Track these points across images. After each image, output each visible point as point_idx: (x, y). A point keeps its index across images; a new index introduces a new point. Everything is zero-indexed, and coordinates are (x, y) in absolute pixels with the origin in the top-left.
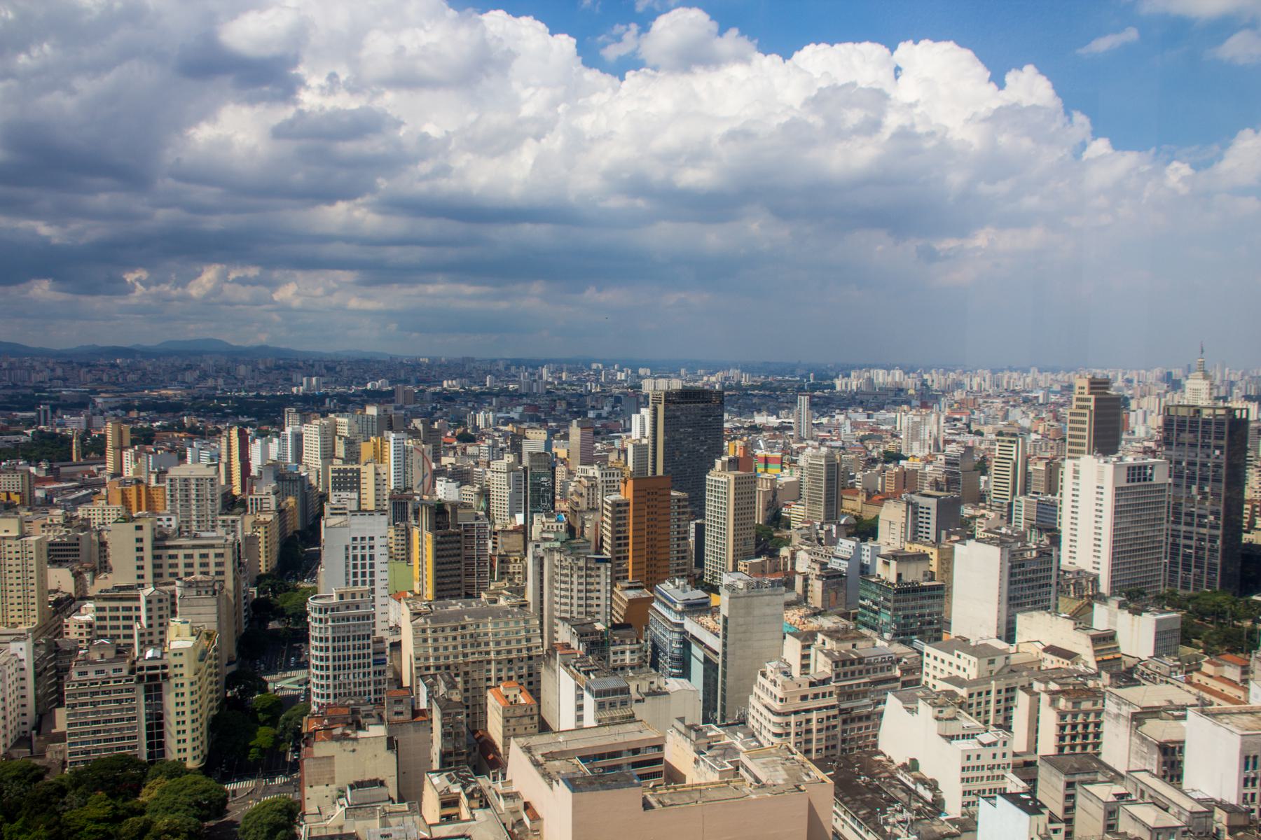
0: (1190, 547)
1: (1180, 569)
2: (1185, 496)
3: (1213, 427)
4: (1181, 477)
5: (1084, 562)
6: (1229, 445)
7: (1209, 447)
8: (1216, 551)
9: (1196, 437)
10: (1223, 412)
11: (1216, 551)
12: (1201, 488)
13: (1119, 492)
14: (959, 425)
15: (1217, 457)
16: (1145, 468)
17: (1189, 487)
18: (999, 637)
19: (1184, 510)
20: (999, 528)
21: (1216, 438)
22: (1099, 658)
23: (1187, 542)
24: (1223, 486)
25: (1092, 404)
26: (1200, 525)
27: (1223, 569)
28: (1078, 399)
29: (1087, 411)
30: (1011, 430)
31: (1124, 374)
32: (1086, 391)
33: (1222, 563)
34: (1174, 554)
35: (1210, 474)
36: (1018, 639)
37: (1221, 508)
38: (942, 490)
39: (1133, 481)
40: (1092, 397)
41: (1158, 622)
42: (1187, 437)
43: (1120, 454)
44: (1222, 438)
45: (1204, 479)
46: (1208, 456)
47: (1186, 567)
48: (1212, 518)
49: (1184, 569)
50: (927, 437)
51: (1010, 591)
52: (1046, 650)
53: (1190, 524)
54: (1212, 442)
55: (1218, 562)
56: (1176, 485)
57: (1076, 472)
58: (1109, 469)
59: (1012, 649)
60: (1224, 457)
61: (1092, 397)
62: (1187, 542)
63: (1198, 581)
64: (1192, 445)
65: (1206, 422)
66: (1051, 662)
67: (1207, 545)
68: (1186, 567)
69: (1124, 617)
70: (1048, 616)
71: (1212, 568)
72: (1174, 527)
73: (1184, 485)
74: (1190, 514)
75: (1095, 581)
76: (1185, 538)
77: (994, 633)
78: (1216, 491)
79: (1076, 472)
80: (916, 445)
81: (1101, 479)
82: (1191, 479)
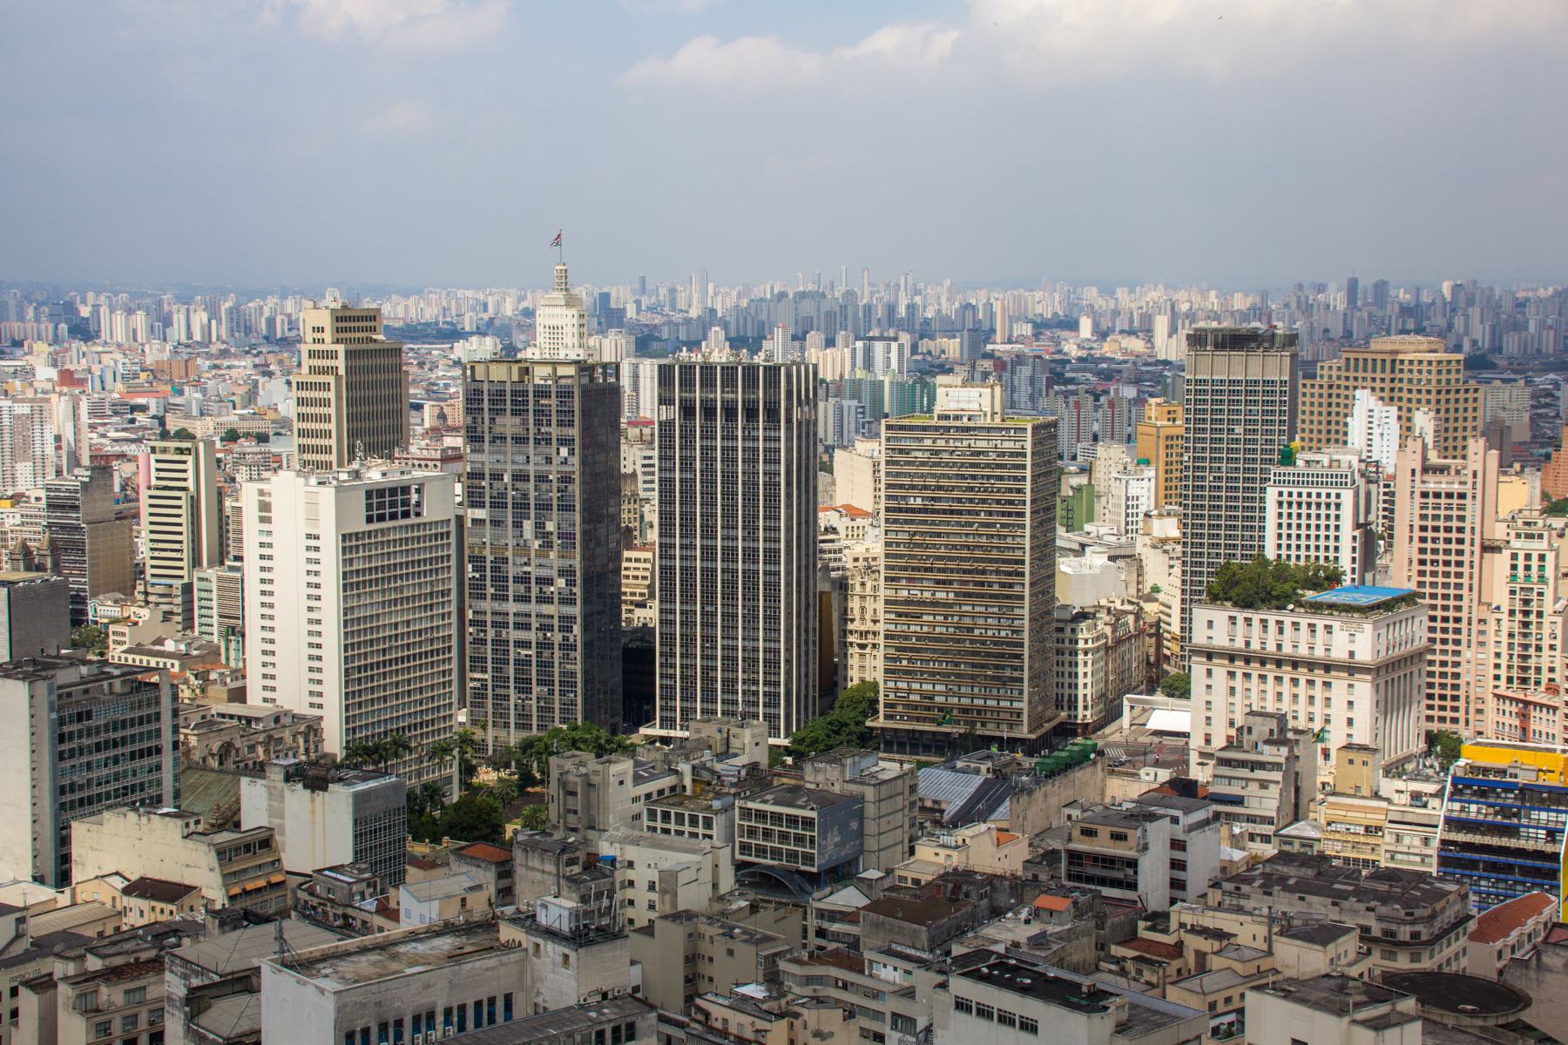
0: (525, 644)
1: (512, 691)
2: (511, 542)
3: (554, 401)
4: (505, 506)
5: (293, 699)
6: (586, 430)
7: (549, 442)
8: (573, 648)
9: (525, 422)
10: (571, 371)
11: (573, 648)
12: (539, 525)
13: (350, 543)
14: (141, 418)
15: (565, 462)
16: (406, 490)
17: (518, 525)
18: (38, 879)
19: (511, 571)
20: (160, 641)
21: (560, 424)
22: (236, 890)
23: (522, 635)
24: (578, 517)
25: (340, 363)
26: (544, 599)
27: (586, 682)
28: (312, 354)
29: (331, 379)
30: (257, 426)
31: (521, 299)
32: (328, 336)
33: (585, 672)
34: (500, 662)
35: (555, 495)
36: (77, 875)
37: (577, 563)
38: (40, 568)
39: (381, 518)
40: (341, 348)
41: (360, 800)
42: (509, 424)
43: (356, 465)
44: (571, 424)
45: (543, 507)
46: (549, 461)
47: (524, 686)
48: (561, 582)
49: (519, 690)
50: (50, 450)
51: (56, 773)
52: (127, 891)
53: (524, 599)
54: (555, 431)
55: (578, 668)
56: (496, 523)
57: (265, 507)
58: (328, 495)
59: (64, 899)
60: (575, 460)
61: (341, 348)
62: (522, 635)
63: (545, 710)
64: (520, 440)
65: (542, 393)
66: (141, 912)
67: (557, 637)
68: (524, 686)
69: (298, 798)
70: (132, 816)
71: (568, 682)
72: (496, 606)
73: (510, 519)
74: (523, 579)
75: (313, 729)
76: (518, 626)
77: (26, 871)
78: (566, 528)
79: (265, 507)
80: (24, 469)
81: (313, 519)
82: (521, 507)
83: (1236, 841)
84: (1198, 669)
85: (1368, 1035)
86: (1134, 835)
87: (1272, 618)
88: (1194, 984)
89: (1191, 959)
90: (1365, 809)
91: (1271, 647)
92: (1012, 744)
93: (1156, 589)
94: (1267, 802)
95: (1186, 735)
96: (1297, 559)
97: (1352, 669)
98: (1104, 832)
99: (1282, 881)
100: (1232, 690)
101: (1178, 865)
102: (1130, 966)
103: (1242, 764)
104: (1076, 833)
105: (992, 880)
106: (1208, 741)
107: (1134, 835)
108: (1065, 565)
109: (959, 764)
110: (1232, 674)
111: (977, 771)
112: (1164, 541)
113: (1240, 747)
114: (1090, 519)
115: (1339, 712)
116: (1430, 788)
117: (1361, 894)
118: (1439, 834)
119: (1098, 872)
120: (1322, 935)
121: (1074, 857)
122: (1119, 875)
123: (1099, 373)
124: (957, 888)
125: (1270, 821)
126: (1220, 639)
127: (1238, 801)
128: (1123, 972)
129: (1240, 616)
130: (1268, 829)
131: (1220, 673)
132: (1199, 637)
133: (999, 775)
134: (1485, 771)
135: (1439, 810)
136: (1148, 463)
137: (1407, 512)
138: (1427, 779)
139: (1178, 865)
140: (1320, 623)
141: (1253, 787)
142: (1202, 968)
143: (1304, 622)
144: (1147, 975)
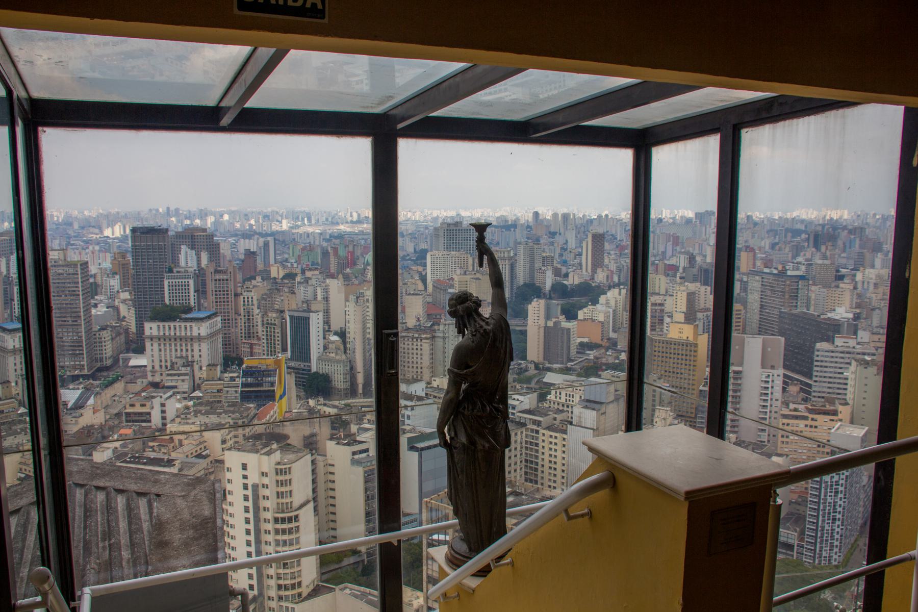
83: (179, 401)
84: (148, 344)
85: (265, 458)
86: (148, 404)
87: (172, 324)
88: (180, 450)
89: (177, 442)
90: (217, 385)
91: (172, 334)
92: (85, 377)
93: (125, 317)
94: (185, 386)
95: (145, 366)
96: (176, 304)
97: (200, 338)
98: (138, 405)
99: (200, 412)
100: (160, 350)
101: (163, 412)
102: (156, 448)
103: (175, 375)
104: (128, 406)
105: (102, 427)
106: (153, 367)
107: (148, 404)
108: (94, 311)
109: (71, 387)
110: (160, 345)
111: (78, 389)
112: (125, 300)
113: (172, 368)
114: (96, 294)
115: (196, 353)
116: (235, 375)
117: (226, 412)
118: (240, 389)
119: (137, 418)
120: (218, 427)
121: (128, 414)
122: (144, 418)
123: (84, 241)
124: (89, 431)
125: (184, 393)
126: (155, 332)
127: (175, 387)
128: (154, 451)
129: (161, 324)
130: (186, 395)
131: (156, 345)
132: (147, 332)
133: (87, 389)
134: (251, 367)
135: (239, 381)
136: (116, 274)
137: (211, 286)
138: (234, 372)
139: (163, 412)
140: (188, 324)
141: (180, 383)
142: (181, 445)
143: (183, 324)
144: (163, 450)
